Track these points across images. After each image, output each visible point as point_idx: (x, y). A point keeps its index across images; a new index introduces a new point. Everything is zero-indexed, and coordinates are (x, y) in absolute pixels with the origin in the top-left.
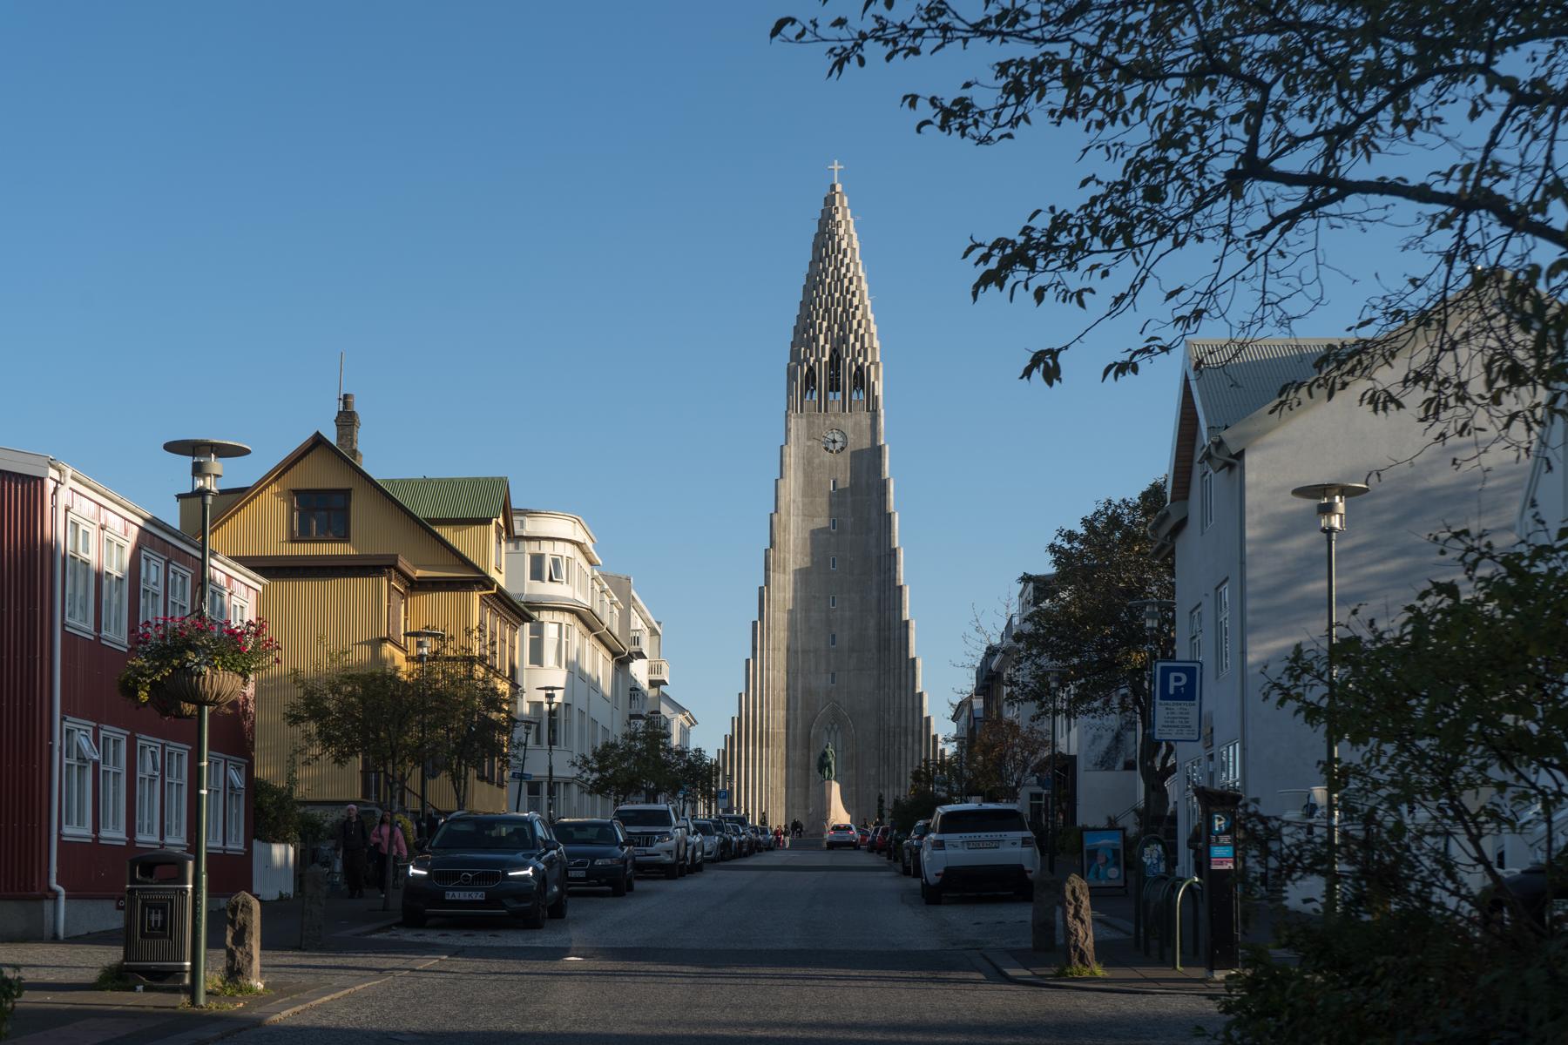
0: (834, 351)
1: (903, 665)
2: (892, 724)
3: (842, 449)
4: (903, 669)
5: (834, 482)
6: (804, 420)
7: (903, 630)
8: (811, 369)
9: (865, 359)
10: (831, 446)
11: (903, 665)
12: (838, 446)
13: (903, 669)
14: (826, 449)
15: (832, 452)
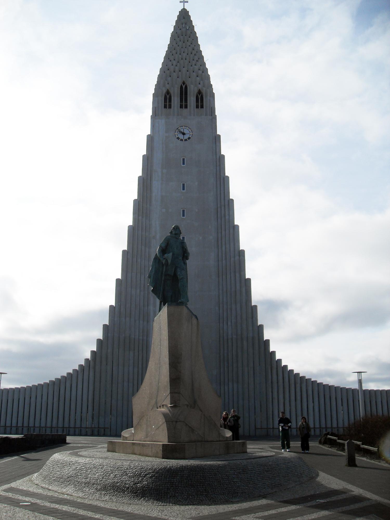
0: (184, 83)
1: (238, 285)
2: (230, 333)
3: (189, 138)
4: (238, 287)
5: (184, 160)
6: (163, 121)
7: (237, 258)
8: (168, 92)
9: (204, 86)
10: (181, 136)
11: (238, 285)
12: (186, 137)
13: (238, 287)
14: (178, 138)
15: (182, 140)
